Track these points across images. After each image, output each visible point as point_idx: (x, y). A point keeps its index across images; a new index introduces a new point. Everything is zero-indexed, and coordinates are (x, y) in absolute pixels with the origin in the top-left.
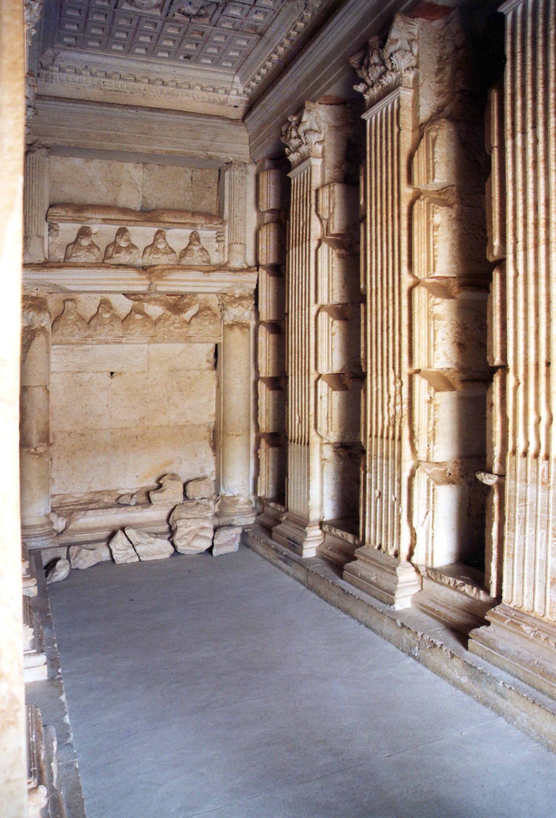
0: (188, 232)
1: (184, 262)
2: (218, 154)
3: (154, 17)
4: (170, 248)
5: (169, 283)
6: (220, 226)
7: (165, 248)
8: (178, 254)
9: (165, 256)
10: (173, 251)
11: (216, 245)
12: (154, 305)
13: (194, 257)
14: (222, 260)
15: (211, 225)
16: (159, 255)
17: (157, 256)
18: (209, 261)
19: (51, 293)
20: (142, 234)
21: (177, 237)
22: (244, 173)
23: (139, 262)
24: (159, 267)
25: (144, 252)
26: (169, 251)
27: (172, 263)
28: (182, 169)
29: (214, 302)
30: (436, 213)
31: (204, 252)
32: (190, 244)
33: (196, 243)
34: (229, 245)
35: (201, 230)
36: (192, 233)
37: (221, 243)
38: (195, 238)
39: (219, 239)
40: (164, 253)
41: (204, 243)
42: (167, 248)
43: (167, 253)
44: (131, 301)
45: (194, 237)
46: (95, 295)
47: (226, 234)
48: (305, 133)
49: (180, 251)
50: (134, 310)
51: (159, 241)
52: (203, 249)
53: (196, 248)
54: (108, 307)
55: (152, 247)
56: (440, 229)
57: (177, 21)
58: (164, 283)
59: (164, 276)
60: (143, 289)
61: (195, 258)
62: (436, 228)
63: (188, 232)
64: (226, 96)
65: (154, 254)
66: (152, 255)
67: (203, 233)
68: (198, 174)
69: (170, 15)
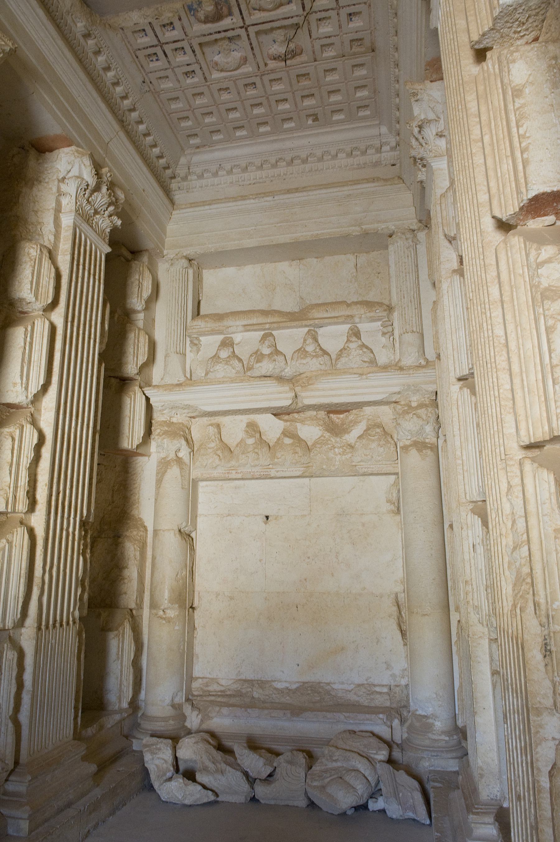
0: (346, 328)
1: (339, 366)
2: (376, 225)
3: (247, 76)
4: (321, 349)
5: (317, 393)
6: (385, 314)
7: (314, 351)
8: (334, 357)
9: (315, 360)
10: (325, 353)
11: (383, 338)
12: (309, 425)
13: (351, 357)
14: (393, 358)
15: (372, 314)
16: (308, 360)
17: (304, 361)
18: (373, 362)
19: (194, 417)
20: (289, 338)
21: (333, 336)
22: (410, 241)
23: (288, 372)
24: (305, 375)
25: (292, 359)
26: (320, 353)
27: (323, 367)
28: (343, 257)
29: (386, 414)
30: (514, 61)
31: (365, 350)
32: (348, 341)
33: (354, 339)
34: (400, 335)
35: (360, 323)
36: (351, 329)
37: (387, 336)
38: (356, 334)
39: (385, 330)
40: (314, 356)
41: (365, 339)
42: (318, 350)
43: (317, 356)
44: (282, 422)
45: (351, 332)
46: (239, 417)
47: (396, 324)
48: (420, 127)
49: (336, 353)
50: (286, 433)
51: (308, 342)
52: (364, 346)
53: (352, 346)
54: (254, 431)
55: (302, 352)
56: (527, 91)
57: (273, 71)
58: (313, 393)
59: (311, 384)
60: (287, 403)
61: (355, 358)
62: (518, 92)
63: (346, 328)
64: (379, 155)
65: (302, 358)
66: (299, 361)
67: (363, 327)
68: (363, 259)
69: (262, 65)
